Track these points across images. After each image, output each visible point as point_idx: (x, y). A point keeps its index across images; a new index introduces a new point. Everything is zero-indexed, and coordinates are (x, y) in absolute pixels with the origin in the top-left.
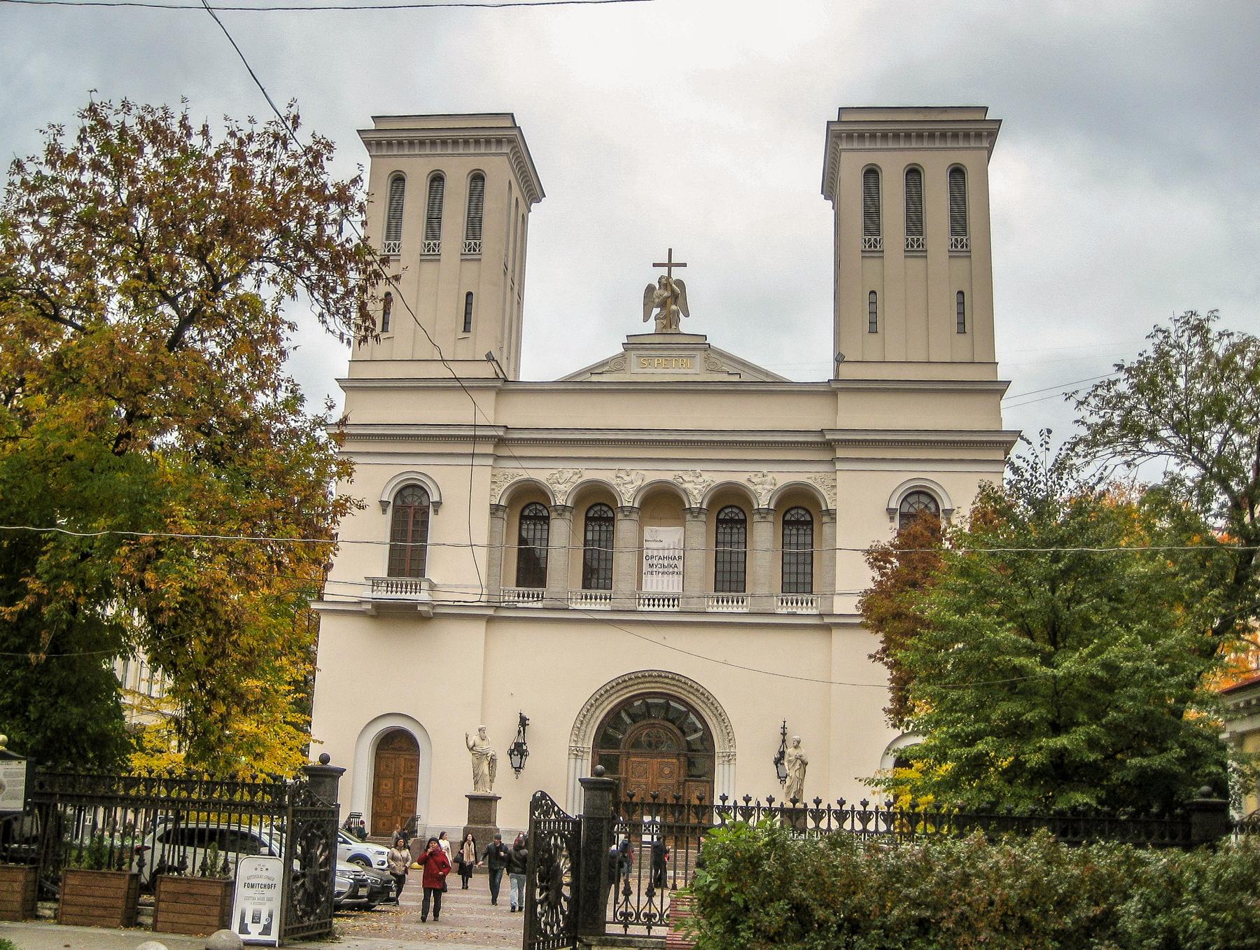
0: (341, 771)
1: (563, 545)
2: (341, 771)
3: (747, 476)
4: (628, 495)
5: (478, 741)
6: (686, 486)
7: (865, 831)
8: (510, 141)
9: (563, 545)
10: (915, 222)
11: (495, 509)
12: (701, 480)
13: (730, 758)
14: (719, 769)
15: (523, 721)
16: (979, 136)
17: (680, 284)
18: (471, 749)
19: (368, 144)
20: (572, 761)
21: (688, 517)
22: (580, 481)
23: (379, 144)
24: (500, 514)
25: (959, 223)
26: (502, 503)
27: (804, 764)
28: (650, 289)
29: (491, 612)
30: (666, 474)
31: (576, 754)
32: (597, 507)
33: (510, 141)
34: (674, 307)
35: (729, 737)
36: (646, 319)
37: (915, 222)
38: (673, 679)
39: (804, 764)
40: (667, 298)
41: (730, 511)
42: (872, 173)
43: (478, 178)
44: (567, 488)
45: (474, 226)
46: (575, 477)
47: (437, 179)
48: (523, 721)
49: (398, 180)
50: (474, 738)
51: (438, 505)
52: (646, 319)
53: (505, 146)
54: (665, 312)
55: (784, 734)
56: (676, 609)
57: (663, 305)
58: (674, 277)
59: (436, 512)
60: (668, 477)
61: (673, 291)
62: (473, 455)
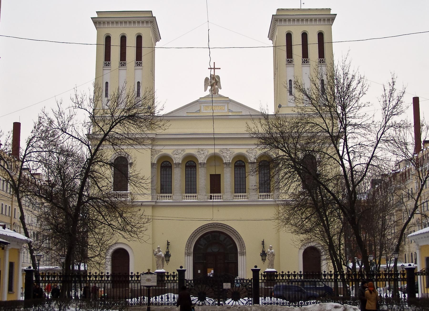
1: (178, 177)
2: (185, 270)
3: (246, 150)
4: (202, 159)
6: (224, 154)
7: (283, 279)
8: (151, 22)
9: (178, 177)
10: (305, 54)
11: (153, 165)
12: (229, 152)
13: (243, 254)
14: (240, 258)
15: (168, 244)
16: (329, 20)
17: (218, 77)
19: (95, 23)
20: (186, 257)
21: (225, 166)
22: (184, 153)
23: (100, 23)
24: (154, 166)
25: (321, 54)
26: (155, 162)
27: (274, 255)
28: (207, 79)
29: (154, 204)
30: (217, 150)
33: (151, 22)
34: (216, 86)
36: (205, 90)
37: (305, 54)
38: (222, 226)
39: (274, 255)
40: (213, 82)
41: (240, 163)
42: (289, 36)
43: (139, 38)
45: (139, 57)
46: (182, 152)
47: (123, 39)
49: (108, 39)
51: (131, 164)
52: (205, 90)
53: (149, 24)
54: (213, 88)
55: (263, 244)
56: (222, 200)
57: (212, 86)
58: (216, 74)
59: (131, 166)
60: (217, 151)
61: (216, 80)
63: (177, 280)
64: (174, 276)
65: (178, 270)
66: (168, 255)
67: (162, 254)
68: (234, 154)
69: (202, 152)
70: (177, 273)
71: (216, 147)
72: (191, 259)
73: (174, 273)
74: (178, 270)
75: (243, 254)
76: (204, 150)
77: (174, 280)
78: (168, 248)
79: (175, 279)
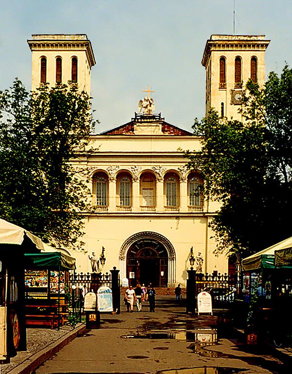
0: (119, 271)
2: (119, 271)
4: (137, 174)
5: (93, 256)
13: (173, 259)
14: (169, 262)
15: (103, 248)
18: (90, 259)
31: (121, 259)
32: (124, 176)
35: (172, 251)
44: (115, 171)
48: (103, 248)
50: (91, 256)
60: (150, 168)
61: (150, 102)
62: (88, 162)
63: (110, 280)
64: (107, 277)
65: (111, 271)
66: (103, 258)
67: (97, 258)
68: (166, 170)
69: (136, 169)
70: (110, 273)
71: (89, 164)
72: (125, 262)
73: (107, 273)
74: (111, 271)
75: (173, 259)
76: (137, 167)
77: (107, 280)
78: (103, 253)
79: (108, 279)
